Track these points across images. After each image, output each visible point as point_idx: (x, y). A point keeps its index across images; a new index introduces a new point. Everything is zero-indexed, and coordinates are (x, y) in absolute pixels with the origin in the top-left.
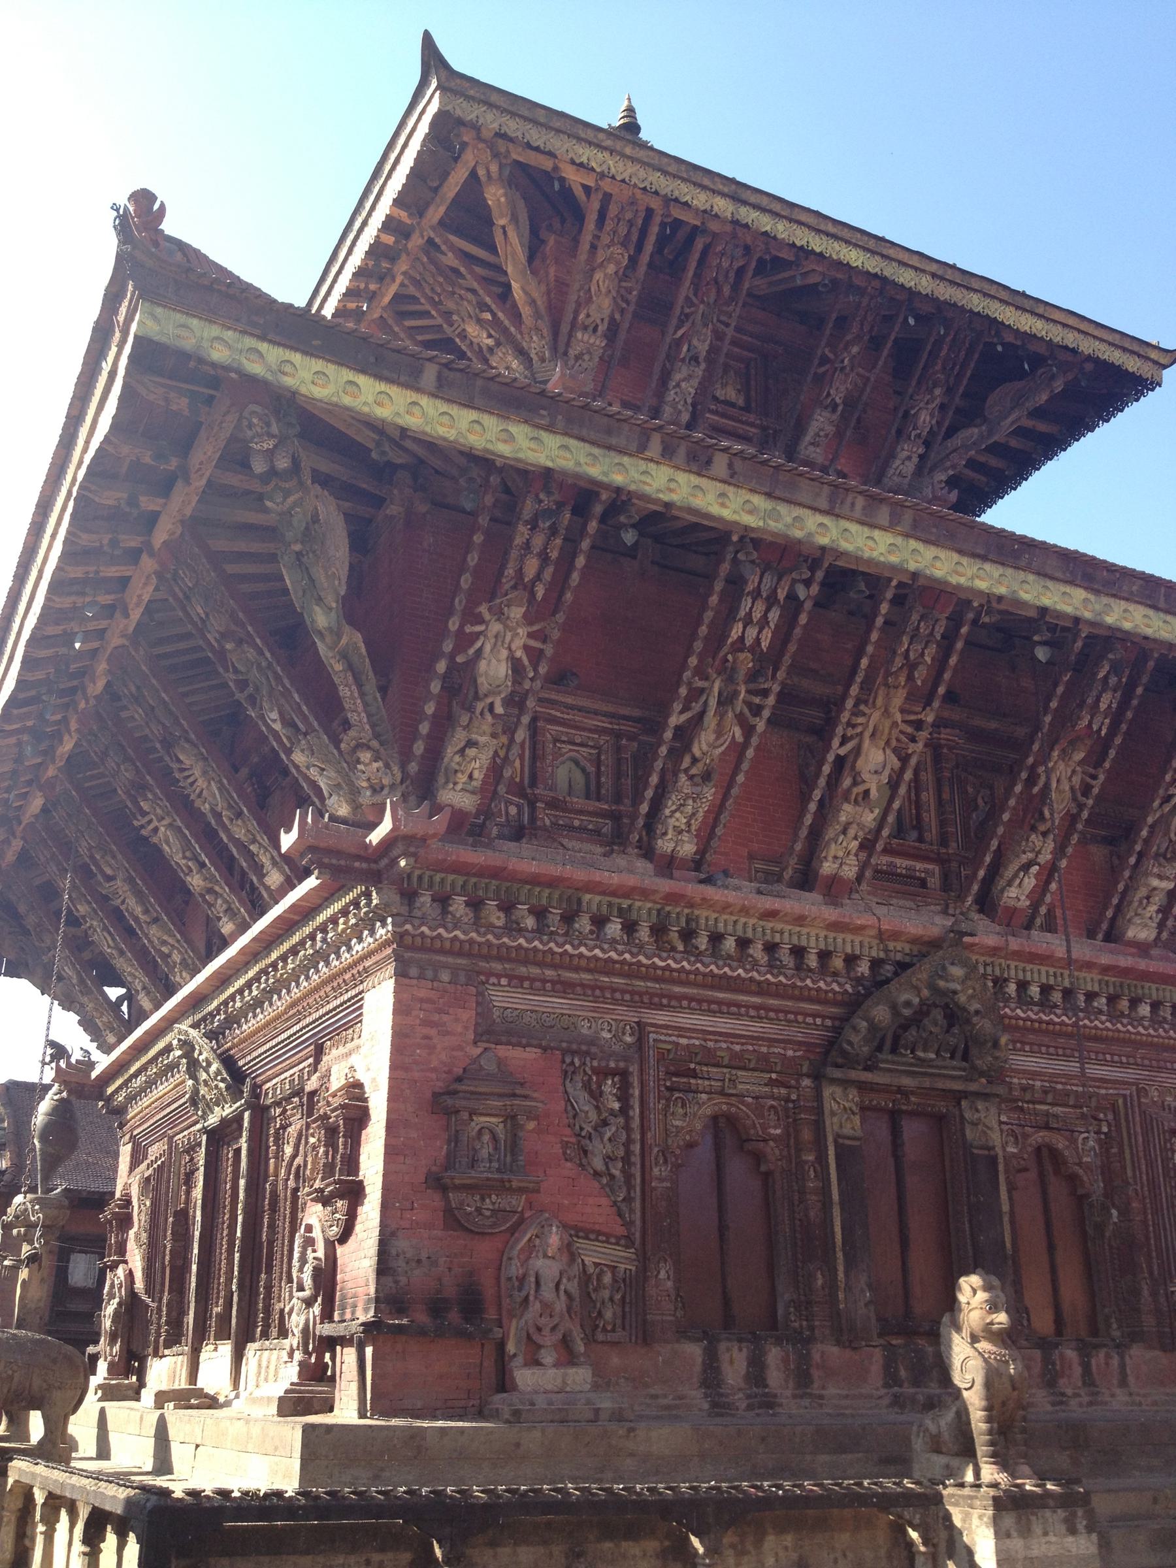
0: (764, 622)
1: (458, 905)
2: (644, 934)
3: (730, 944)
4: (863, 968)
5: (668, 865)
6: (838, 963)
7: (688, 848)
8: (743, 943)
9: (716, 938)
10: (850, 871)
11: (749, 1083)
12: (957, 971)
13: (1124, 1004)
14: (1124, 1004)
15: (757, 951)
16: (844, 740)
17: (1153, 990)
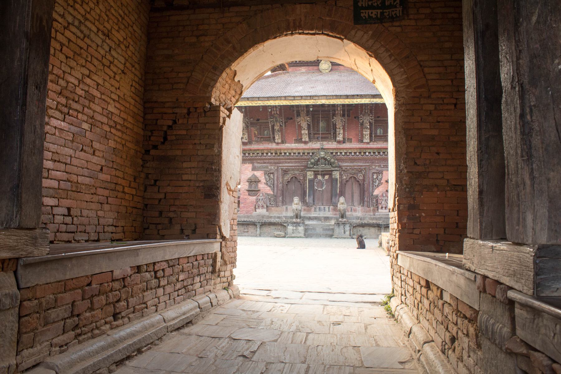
0: (276, 111)
1: (247, 155)
2: (274, 154)
3: (288, 154)
4: (311, 154)
5: (278, 143)
6: (306, 154)
7: (280, 141)
8: (290, 153)
9: (285, 153)
10: (307, 139)
11: (296, 172)
12: (322, 153)
13: (362, 154)
14: (362, 154)
15: (292, 154)
16: (298, 122)
17: (369, 151)
